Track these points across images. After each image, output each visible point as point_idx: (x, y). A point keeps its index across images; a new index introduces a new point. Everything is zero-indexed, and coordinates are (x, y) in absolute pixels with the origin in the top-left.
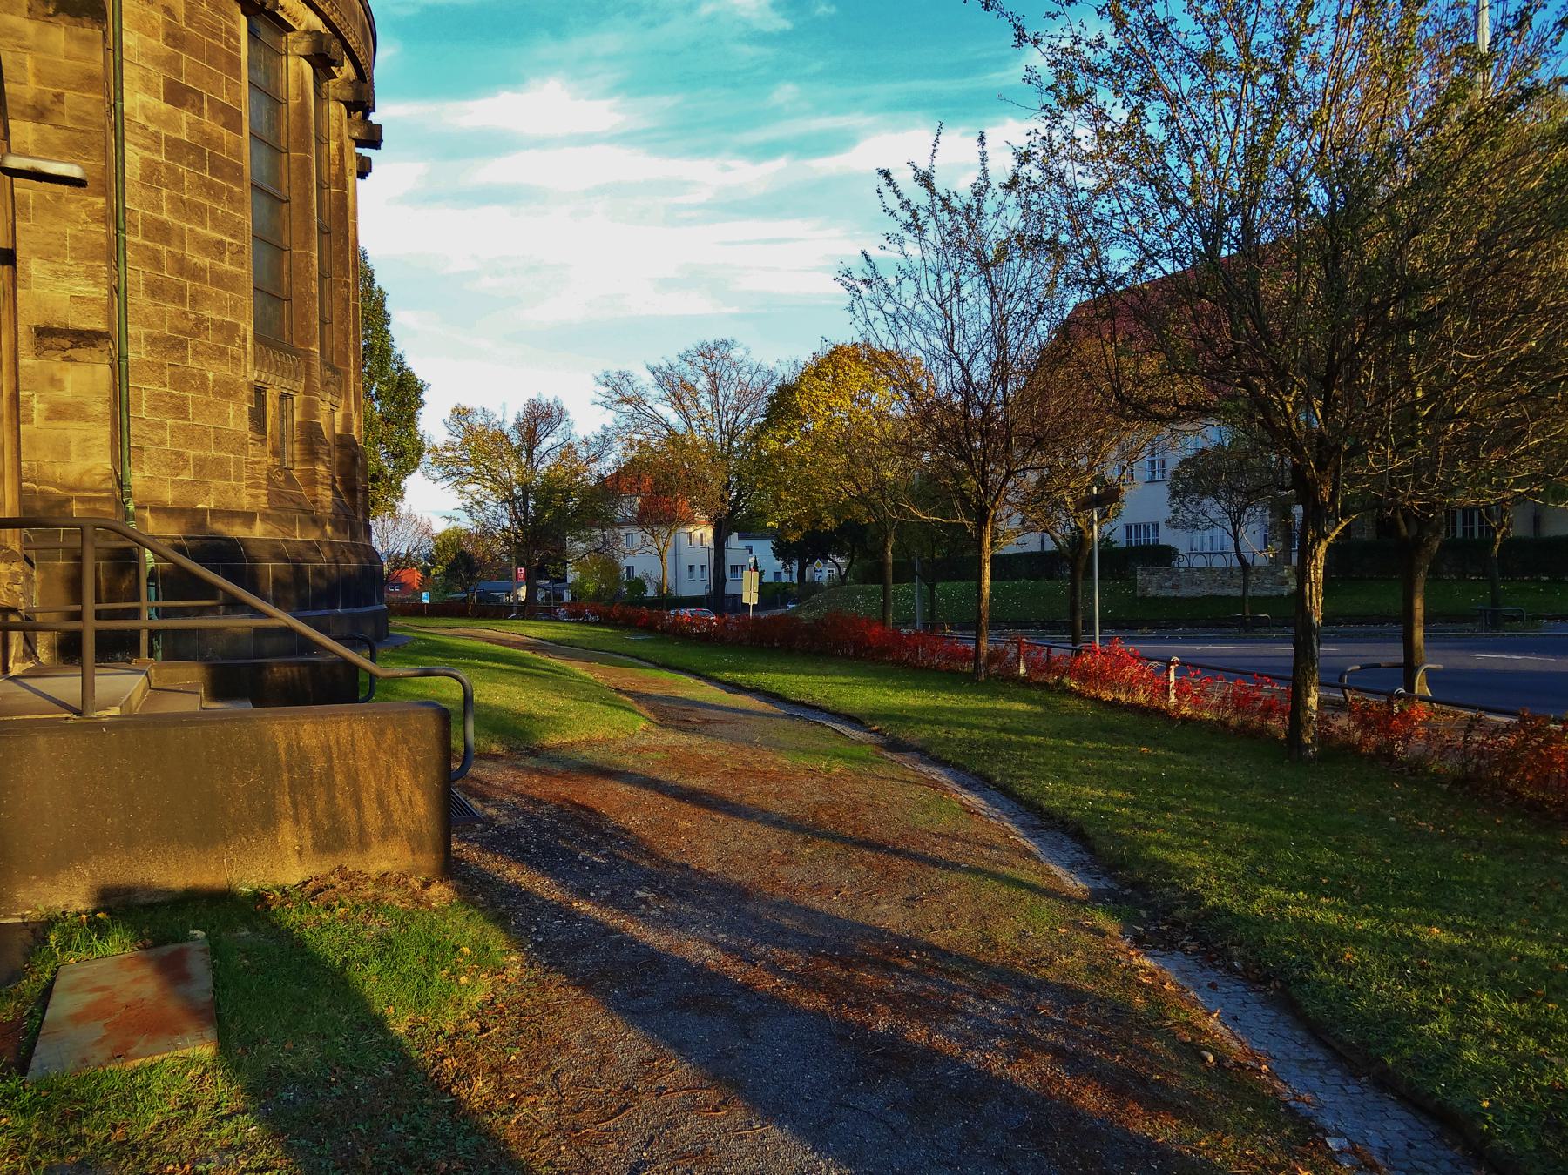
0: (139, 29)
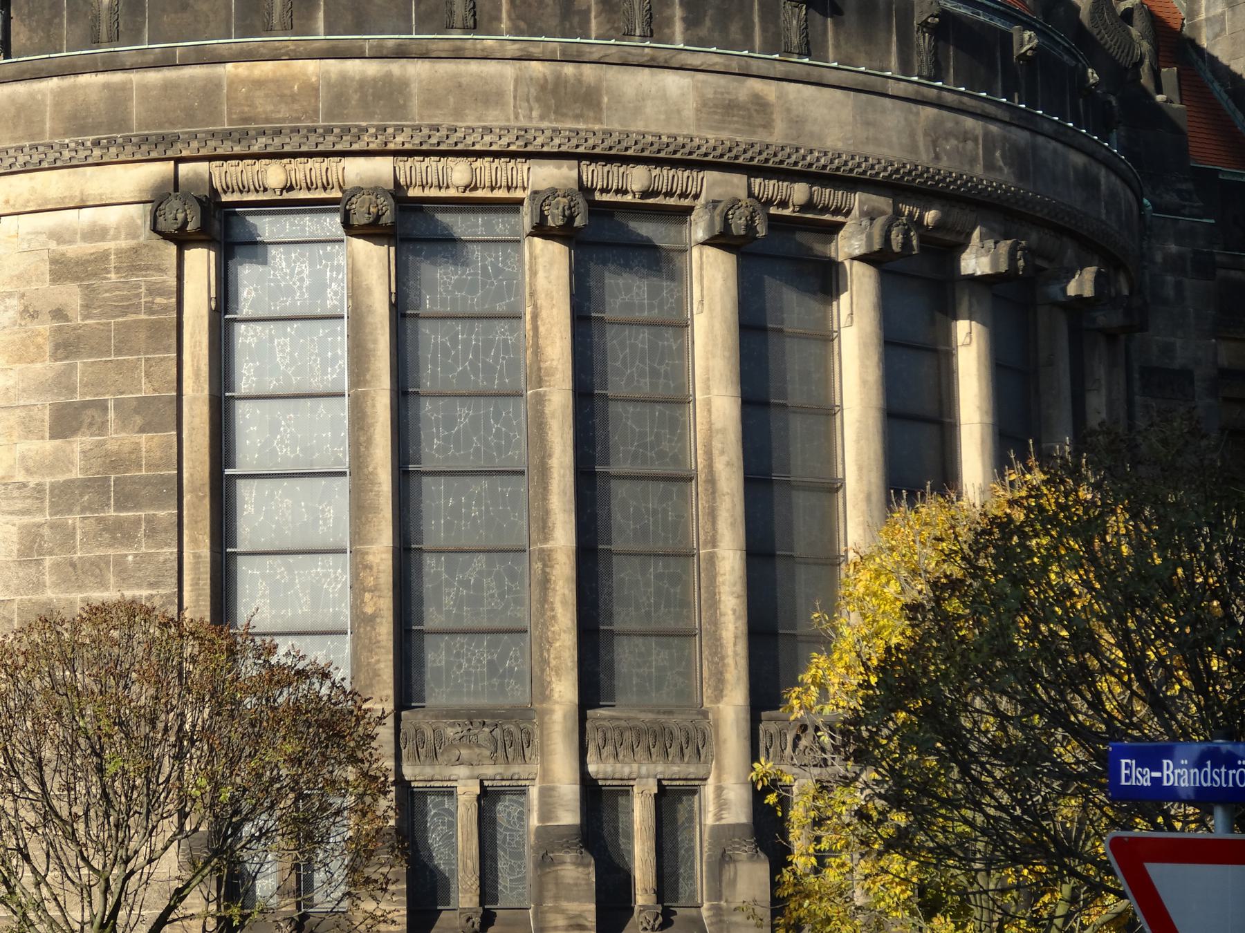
0: (20, 359)
